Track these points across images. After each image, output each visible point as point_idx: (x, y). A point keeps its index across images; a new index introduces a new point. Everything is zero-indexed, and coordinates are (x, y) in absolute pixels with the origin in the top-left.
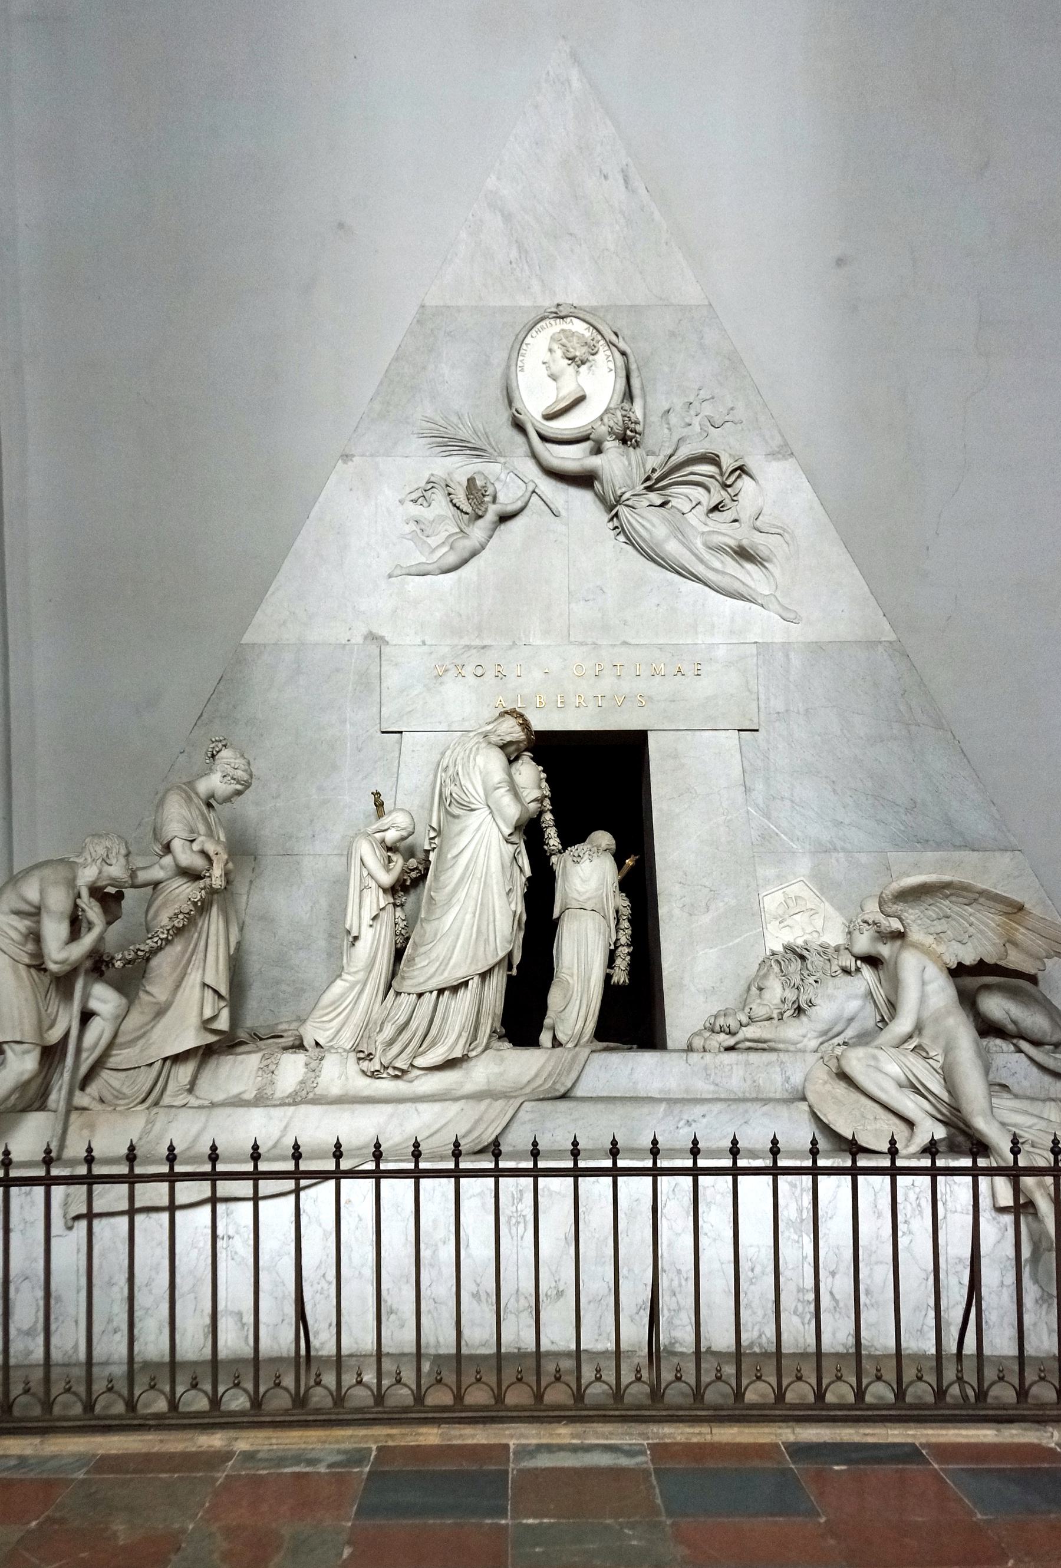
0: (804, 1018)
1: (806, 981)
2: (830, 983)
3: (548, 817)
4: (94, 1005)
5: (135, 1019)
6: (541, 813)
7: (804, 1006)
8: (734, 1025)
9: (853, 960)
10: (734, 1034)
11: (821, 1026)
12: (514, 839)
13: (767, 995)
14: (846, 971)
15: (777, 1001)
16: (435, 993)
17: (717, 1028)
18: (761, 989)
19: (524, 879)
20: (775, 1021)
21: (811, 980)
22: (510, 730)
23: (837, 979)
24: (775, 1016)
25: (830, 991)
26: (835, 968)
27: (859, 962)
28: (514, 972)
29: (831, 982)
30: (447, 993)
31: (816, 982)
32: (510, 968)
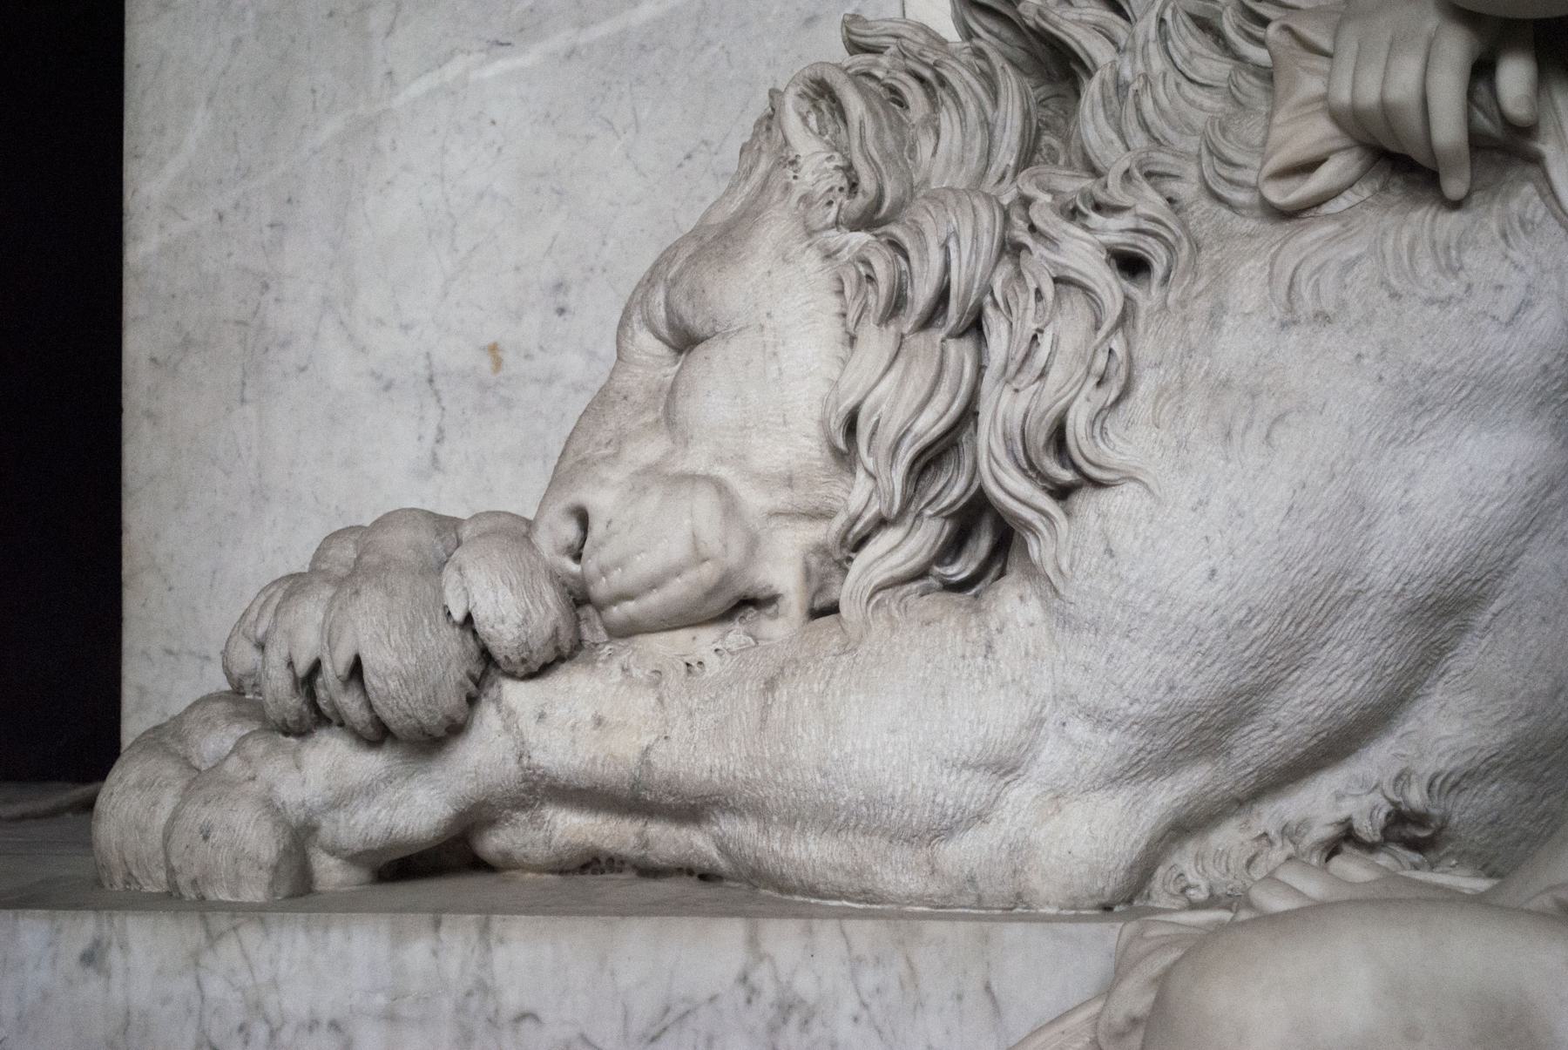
0: (1013, 603)
1: (1039, 263)
2: (1248, 284)
7: (1014, 490)
8: (399, 653)
9: (1455, 48)
10: (432, 740)
11: (1148, 673)
13: (717, 389)
14: (1396, 161)
15: (800, 445)
17: (279, 687)
18: (684, 341)
20: (780, 628)
21: (1082, 252)
23: (1313, 234)
24: (782, 571)
25: (1236, 346)
26: (1314, 133)
27: (1515, 78)
29: (1252, 269)
31: (1131, 265)
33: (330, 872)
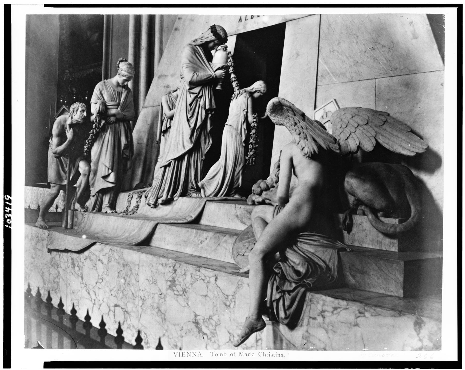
3: (233, 76)
4: (81, 170)
5: (91, 176)
6: (228, 75)
12: (192, 91)
16: (163, 168)
19: (204, 111)
22: (207, 36)
28: (204, 158)
30: (168, 168)
32: (202, 157)
33: (256, 203)
